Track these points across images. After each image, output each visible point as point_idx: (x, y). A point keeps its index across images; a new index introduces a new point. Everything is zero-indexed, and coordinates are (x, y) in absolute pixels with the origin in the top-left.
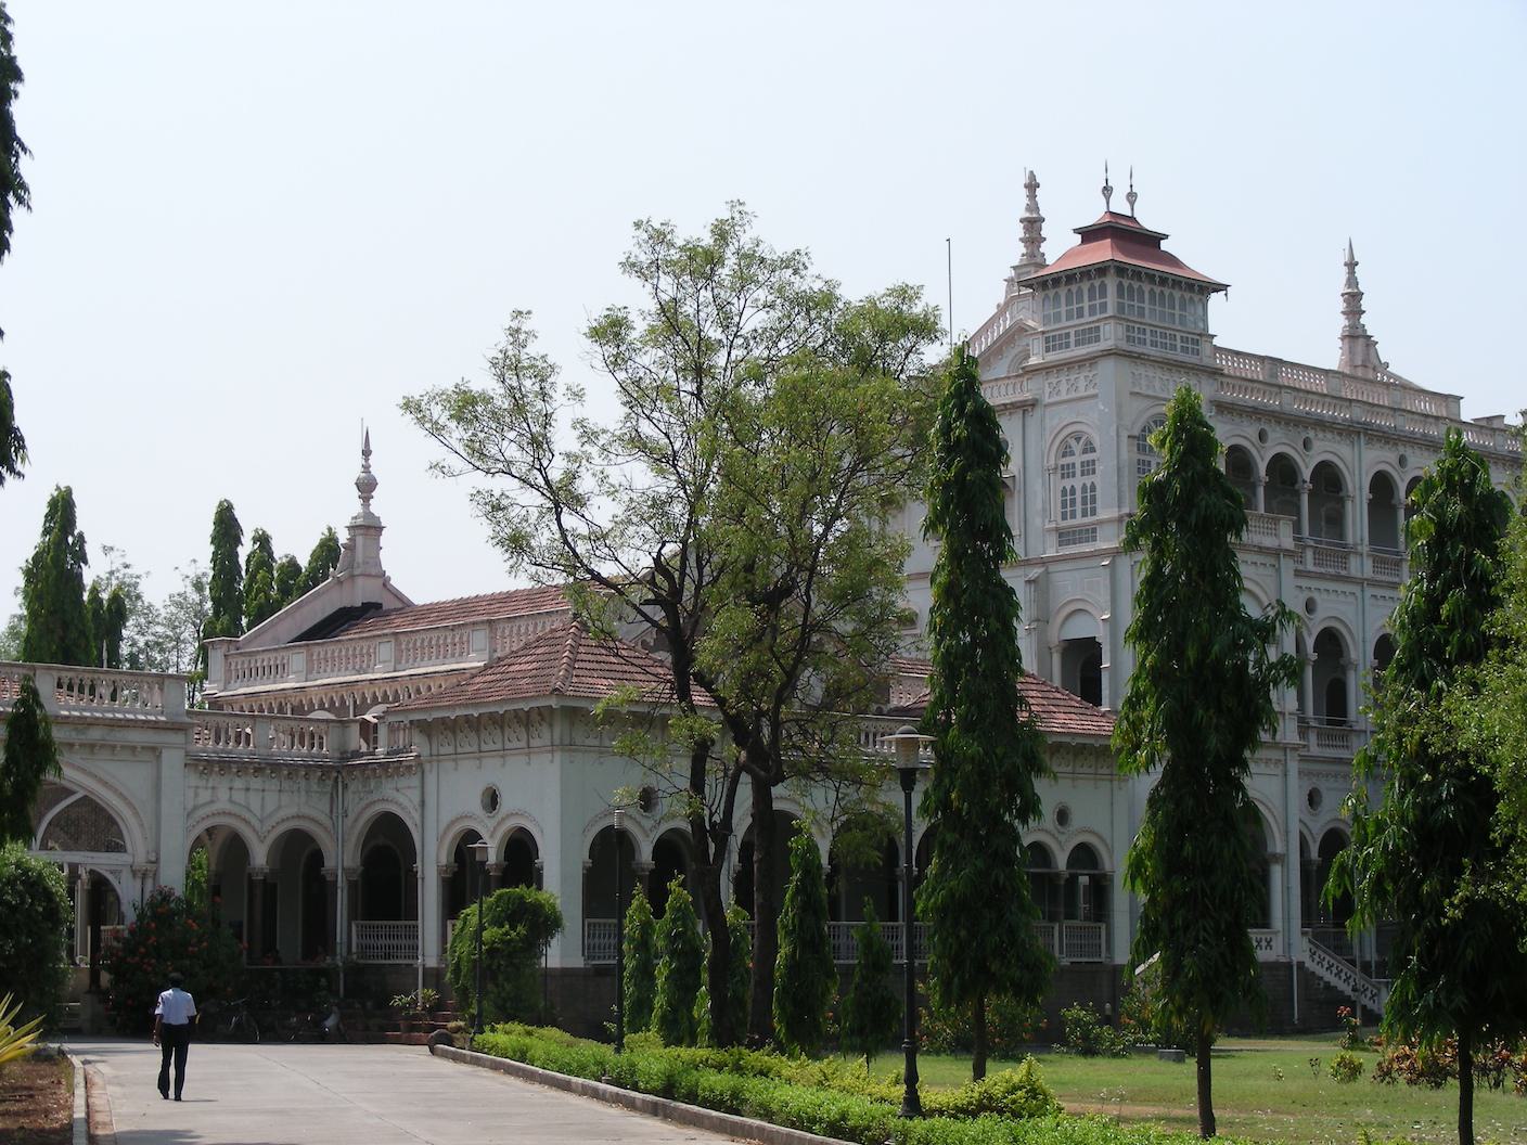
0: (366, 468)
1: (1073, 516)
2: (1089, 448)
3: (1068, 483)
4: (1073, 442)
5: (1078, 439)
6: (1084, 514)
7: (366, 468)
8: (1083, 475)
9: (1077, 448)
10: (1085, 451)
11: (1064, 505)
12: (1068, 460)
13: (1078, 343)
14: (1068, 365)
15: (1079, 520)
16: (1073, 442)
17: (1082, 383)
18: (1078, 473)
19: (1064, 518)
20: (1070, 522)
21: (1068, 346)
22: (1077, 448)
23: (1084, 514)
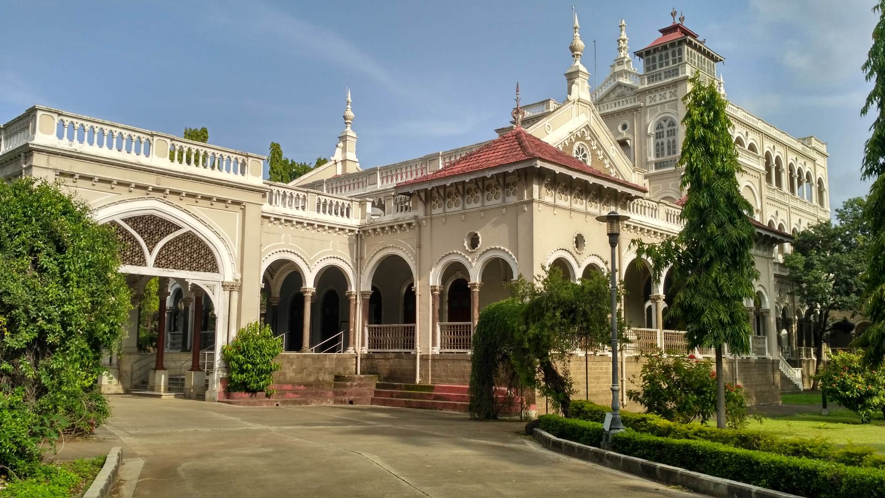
3: (660, 141)
4: (663, 122)
5: (665, 121)
6: (669, 154)
8: (668, 136)
9: (665, 125)
11: (657, 150)
12: (660, 130)
13: (666, 77)
14: (656, 89)
15: (666, 157)
16: (663, 122)
17: (668, 95)
21: (660, 79)
22: (665, 125)
23: (669, 154)
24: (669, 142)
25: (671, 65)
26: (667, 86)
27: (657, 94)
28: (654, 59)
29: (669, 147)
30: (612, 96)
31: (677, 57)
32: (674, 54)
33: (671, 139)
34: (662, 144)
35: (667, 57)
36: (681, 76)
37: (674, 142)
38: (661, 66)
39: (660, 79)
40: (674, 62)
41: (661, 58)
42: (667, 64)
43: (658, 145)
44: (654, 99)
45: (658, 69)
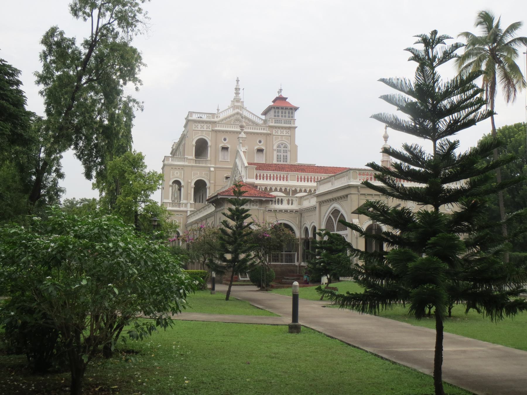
0: (386, 132)
1: (280, 161)
2: (286, 147)
3: (279, 154)
6: (284, 161)
7: (386, 132)
10: (284, 148)
11: (278, 158)
13: (284, 123)
14: (279, 128)
15: (282, 163)
17: (285, 132)
18: (282, 151)
19: (278, 161)
20: (279, 163)
22: (282, 146)
24: (284, 156)
25: (287, 118)
26: (286, 128)
27: (279, 130)
28: (278, 112)
29: (284, 159)
30: (224, 121)
31: (291, 115)
32: (289, 113)
33: (285, 154)
34: (280, 156)
35: (285, 113)
36: (293, 125)
37: (286, 156)
38: (282, 116)
39: (281, 123)
40: (289, 117)
41: (282, 113)
42: (285, 116)
43: (278, 156)
44: (277, 132)
45: (280, 117)
